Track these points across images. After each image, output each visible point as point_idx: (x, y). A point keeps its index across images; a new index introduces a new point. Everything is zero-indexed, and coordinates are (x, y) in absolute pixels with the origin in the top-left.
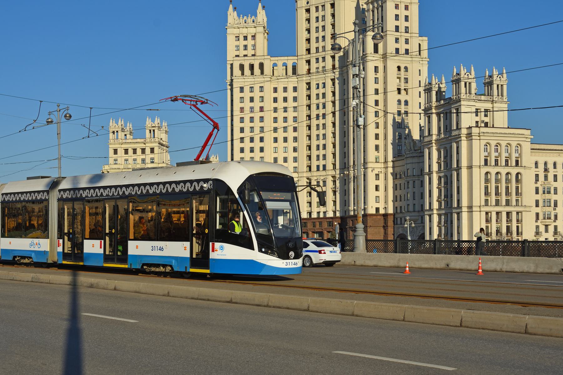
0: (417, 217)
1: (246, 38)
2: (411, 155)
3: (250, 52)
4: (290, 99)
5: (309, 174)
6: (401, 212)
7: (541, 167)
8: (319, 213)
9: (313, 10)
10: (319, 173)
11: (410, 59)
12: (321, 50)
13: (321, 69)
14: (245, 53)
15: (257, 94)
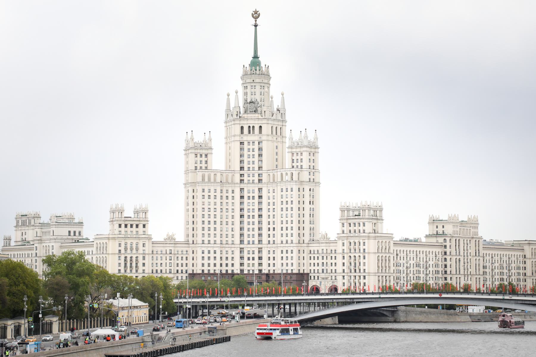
0: (328, 276)
1: (201, 155)
2: (325, 242)
3: (204, 165)
4: (230, 198)
5: (242, 246)
6: (314, 272)
7: (395, 252)
8: (249, 270)
9: (246, 143)
10: (249, 246)
11: (315, 184)
12: (251, 169)
13: (251, 181)
14: (201, 165)
15: (212, 194)
